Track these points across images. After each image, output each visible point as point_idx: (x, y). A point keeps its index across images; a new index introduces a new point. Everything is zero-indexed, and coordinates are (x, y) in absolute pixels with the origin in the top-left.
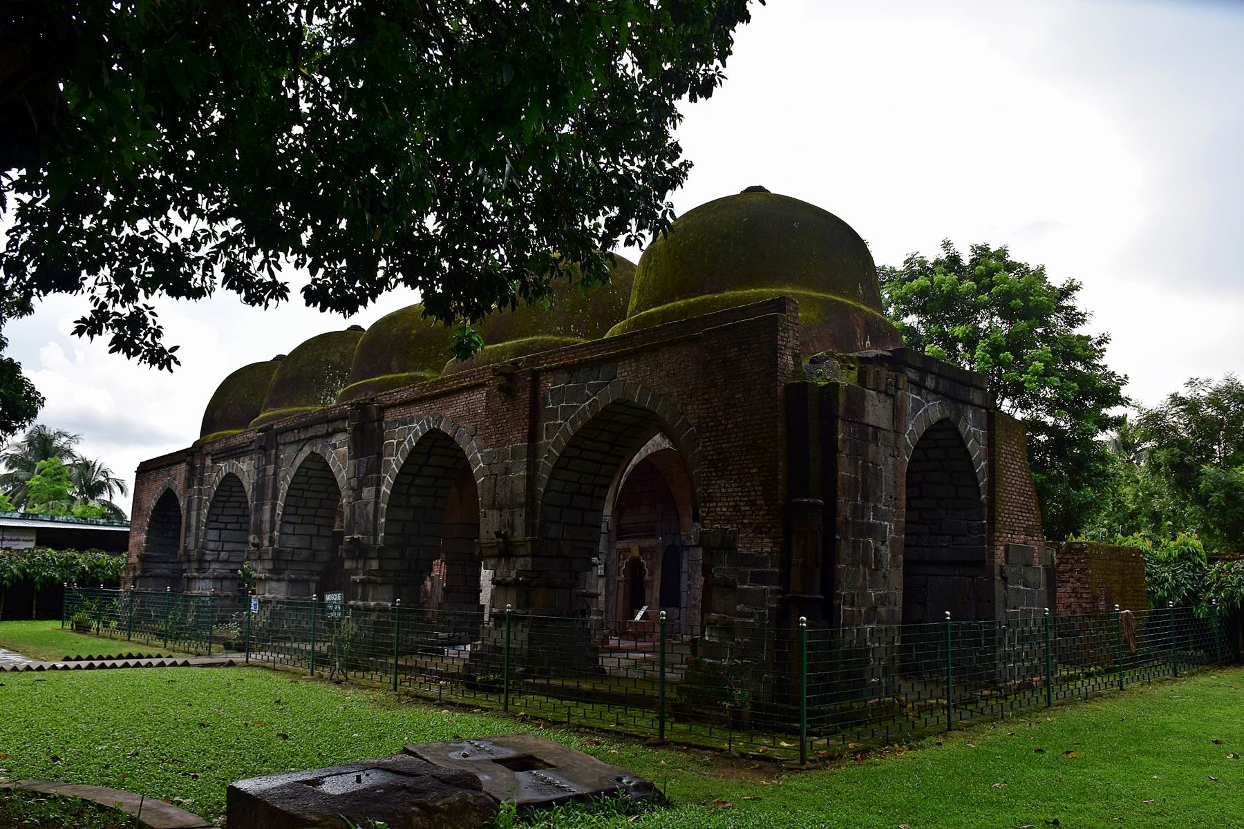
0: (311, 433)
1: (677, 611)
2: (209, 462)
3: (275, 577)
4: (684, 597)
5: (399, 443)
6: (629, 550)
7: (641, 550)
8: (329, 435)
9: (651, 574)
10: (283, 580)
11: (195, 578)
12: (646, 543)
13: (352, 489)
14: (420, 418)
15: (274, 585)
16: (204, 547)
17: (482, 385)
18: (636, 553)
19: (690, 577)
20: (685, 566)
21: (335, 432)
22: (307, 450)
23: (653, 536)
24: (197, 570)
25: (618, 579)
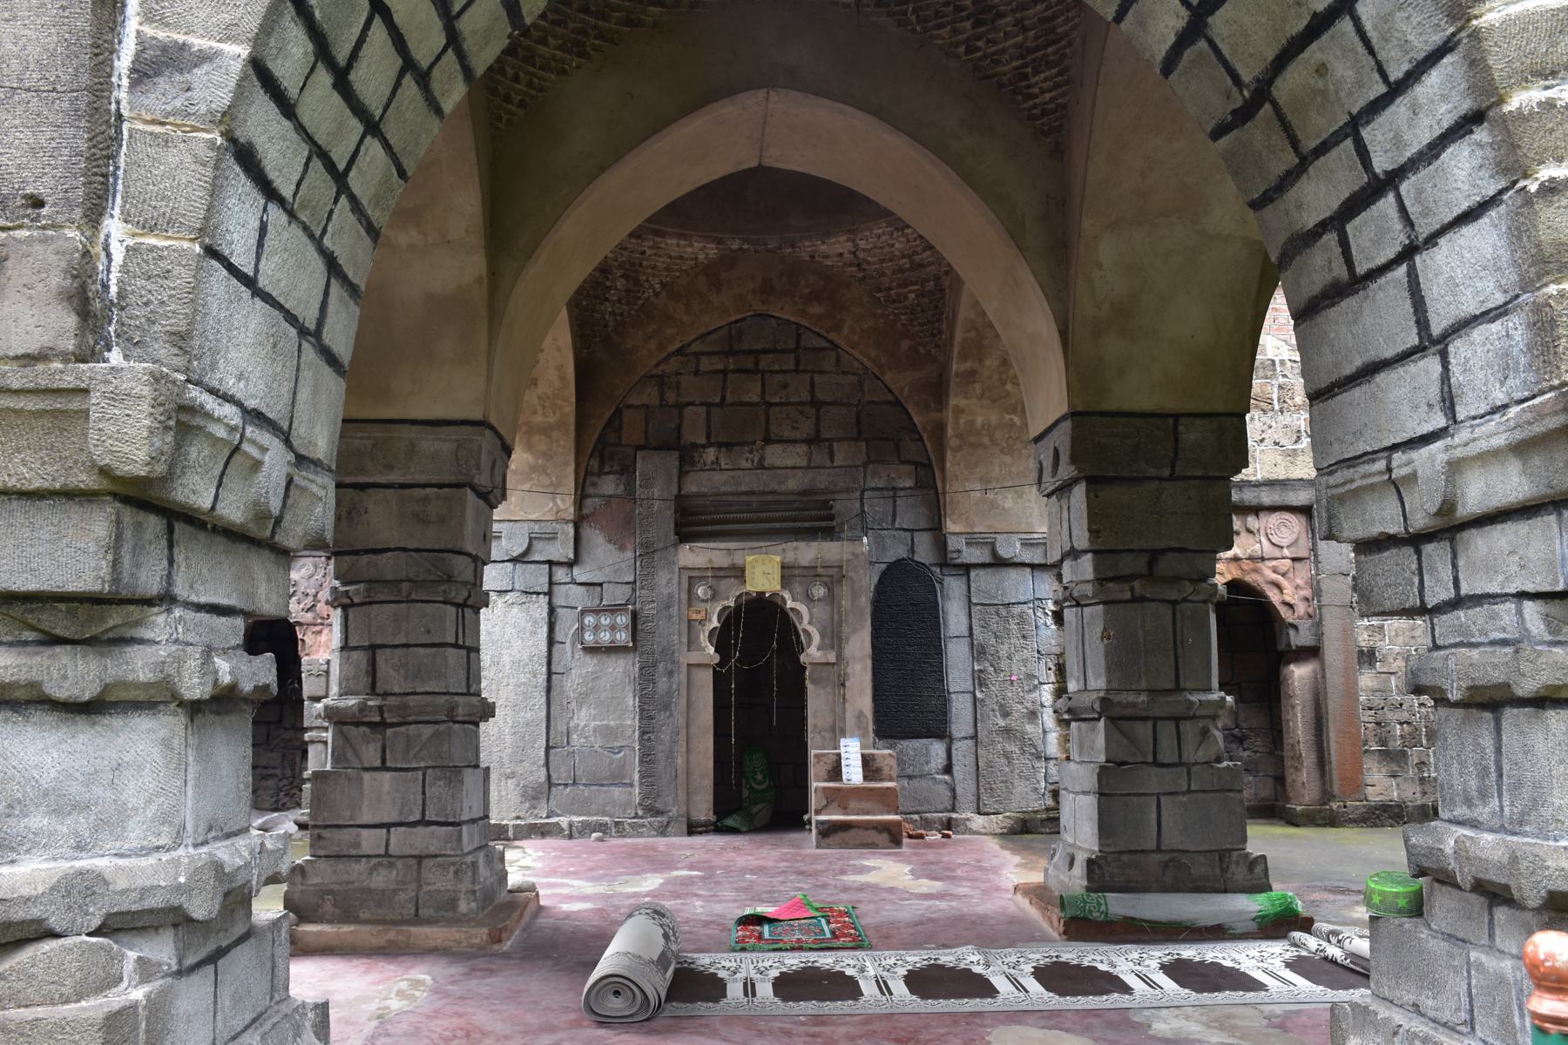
1: (937, 748)
3: (74, 673)
4: (960, 709)
6: (739, 573)
7: (788, 573)
9: (835, 639)
10: (151, 699)
12: (807, 552)
18: (763, 572)
19: (978, 652)
20: (955, 618)
23: (829, 533)
25: (694, 658)
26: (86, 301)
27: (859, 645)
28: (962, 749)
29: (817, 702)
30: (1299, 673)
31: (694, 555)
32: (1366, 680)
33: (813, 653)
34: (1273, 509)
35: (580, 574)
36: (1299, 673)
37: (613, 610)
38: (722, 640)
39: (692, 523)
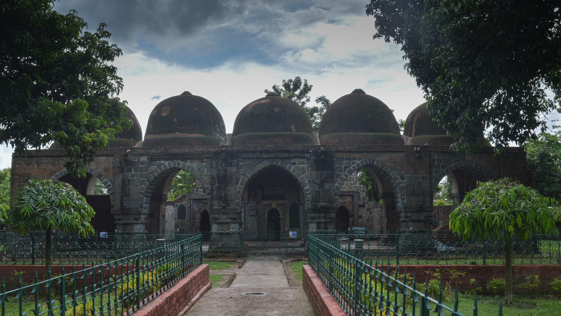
0: (272, 155)
1: (298, 229)
2: (144, 159)
3: (235, 221)
4: (302, 224)
5: (346, 168)
6: (271, 205)
7: (278, 205)
8: (289, 158)
11: (135, 223)
13: (317, 184)
14: (361, 159)
15: (233, 225)
16: (142, 207)
17: (403, 152)
18: (274, 206)
20: (301, 211)
21: (294, 157)
22: (267, 163)
24: (136, 219)
26: (236, 204)
27: (288, 215)
28: (302, 229)
29: (282, 223)
30: (351, 219)
31: (265, 202)
32: (360, 220)
33: (281, 216)
34: (347, 195)
35: (249, 205)
36: (351, 219)
37: (253, 210)
38: (268, 214)
39: (264, 198)
